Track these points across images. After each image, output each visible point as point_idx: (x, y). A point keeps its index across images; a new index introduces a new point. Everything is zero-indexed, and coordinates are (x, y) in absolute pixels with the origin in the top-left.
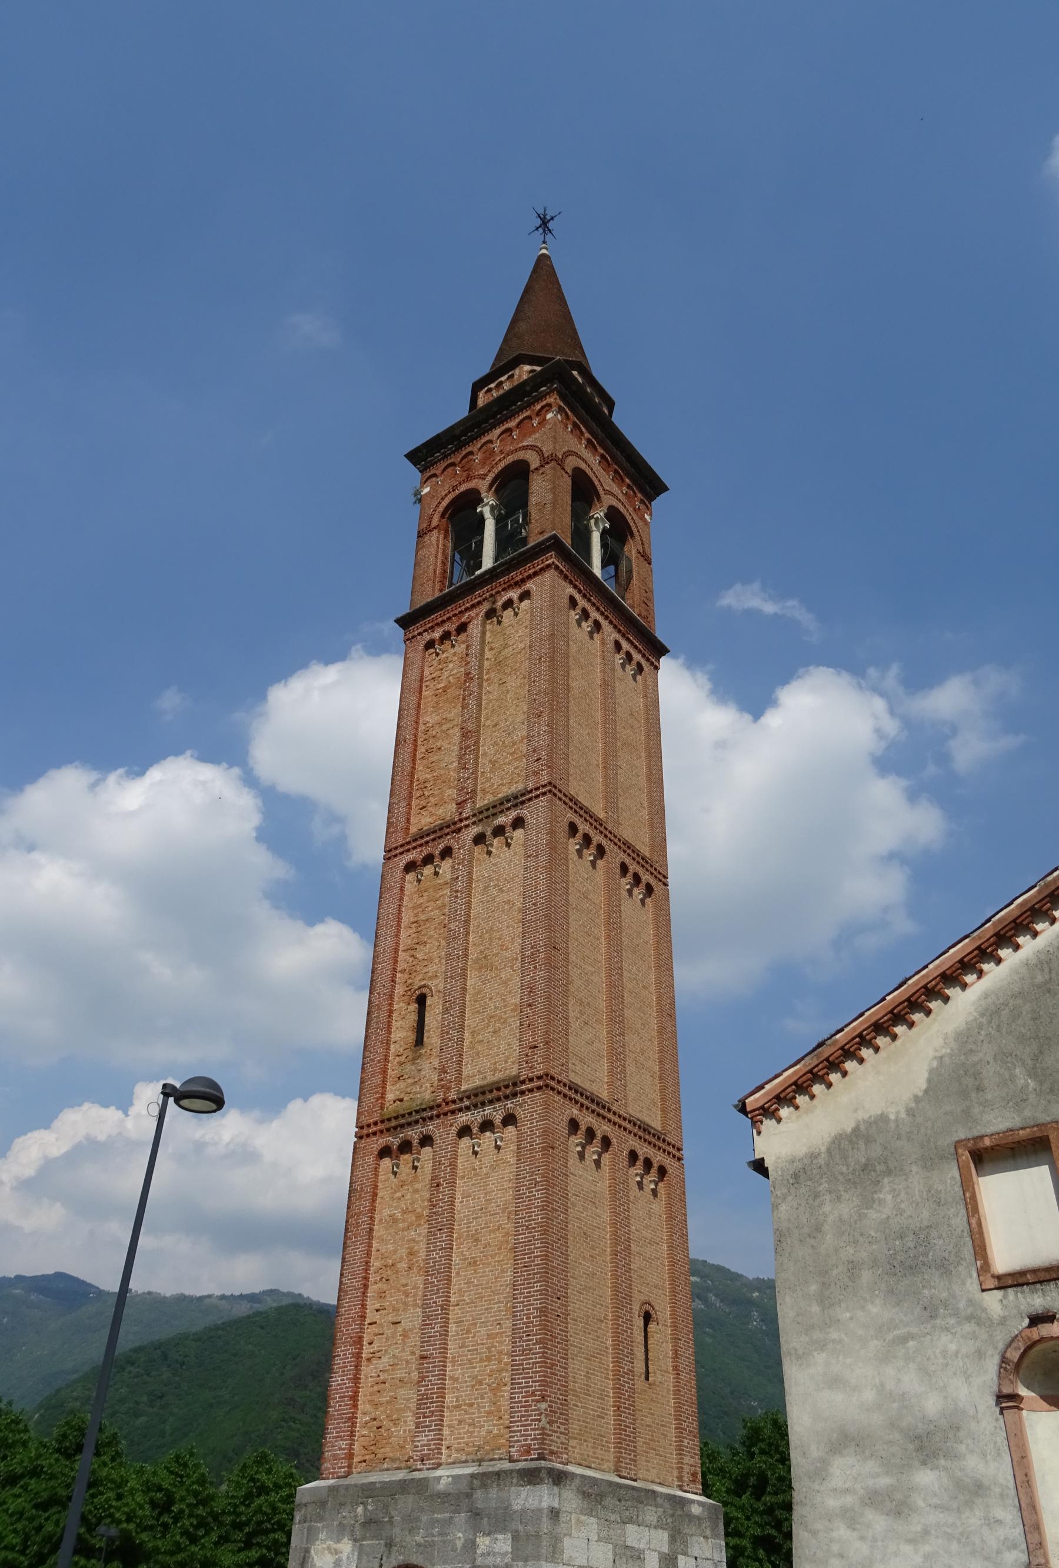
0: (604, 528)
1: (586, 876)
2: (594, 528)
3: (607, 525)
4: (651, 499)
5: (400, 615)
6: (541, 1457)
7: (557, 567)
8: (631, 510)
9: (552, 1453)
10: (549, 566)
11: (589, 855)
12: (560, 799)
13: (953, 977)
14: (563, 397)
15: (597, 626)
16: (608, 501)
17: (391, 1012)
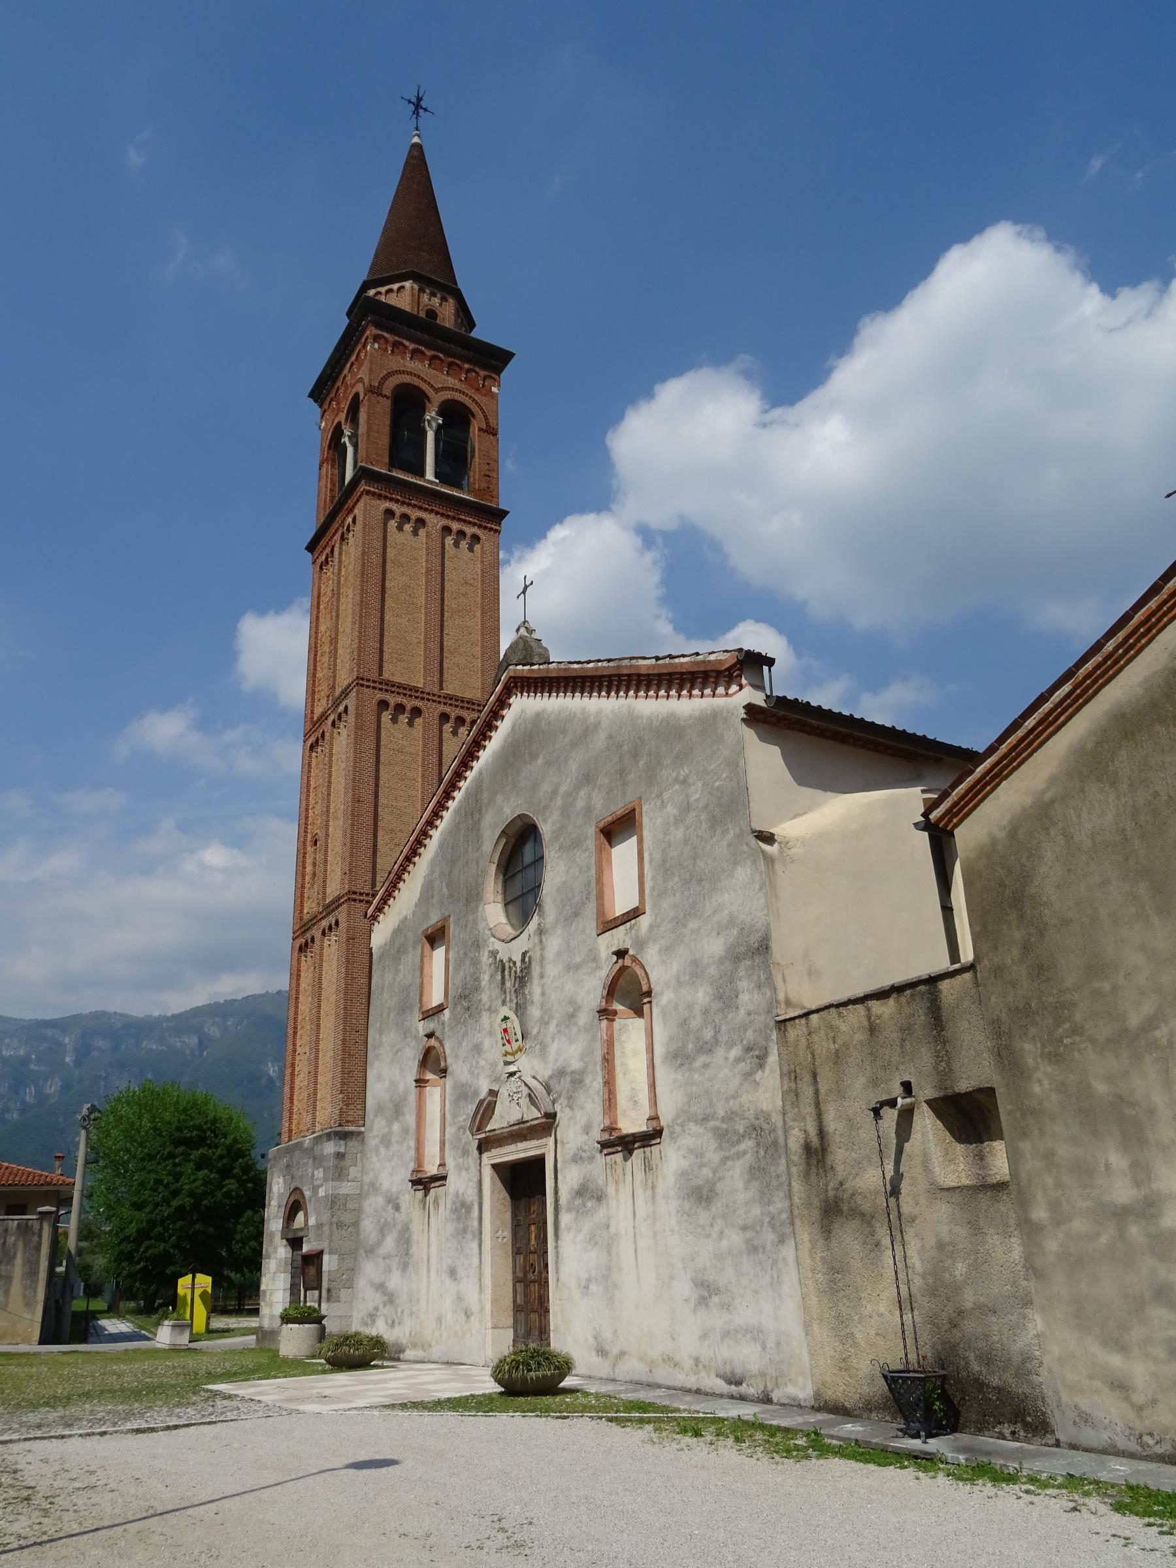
0: (439, 426)
1: (401, 736)
2: (428, 429)
3: (441, 422)
4: (499, 373)
5: (306, 544)
6: (340, 1125)
7: (368, 492)
8: (471, 392)
9: (348, 1121)
10: (362, 493)
11: (404, 719)
12: (368, 687)
13: (430, 823)
14: (378, 325)
15: (421, 522)
16: (437, 399)
17: (305, 853)
